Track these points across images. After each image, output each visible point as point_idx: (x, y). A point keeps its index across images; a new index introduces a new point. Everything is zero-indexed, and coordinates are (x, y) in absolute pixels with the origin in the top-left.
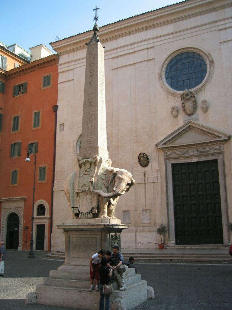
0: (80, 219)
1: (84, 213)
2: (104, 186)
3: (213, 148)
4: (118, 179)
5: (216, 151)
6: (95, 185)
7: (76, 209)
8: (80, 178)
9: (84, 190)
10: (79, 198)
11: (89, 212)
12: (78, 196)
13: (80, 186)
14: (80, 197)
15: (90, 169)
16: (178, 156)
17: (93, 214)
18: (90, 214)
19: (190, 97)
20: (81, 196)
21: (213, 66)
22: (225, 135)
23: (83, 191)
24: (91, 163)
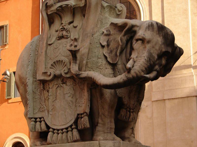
0: (50, 144)
1: (58, 130)
2: (104, 62)
4: (140, 42)
6: (81, 62)
7: (41, 122)
8: (49, 47)
9: (58, 72)
10: (46, 96)
11: (71, 126)
12: (44, 88)
13: (49, 66)
14: (48, 91)
15: (72, 24)
17: (80, 132)
18: (72, 131)
20: (50, 90)
23: (55, 75)
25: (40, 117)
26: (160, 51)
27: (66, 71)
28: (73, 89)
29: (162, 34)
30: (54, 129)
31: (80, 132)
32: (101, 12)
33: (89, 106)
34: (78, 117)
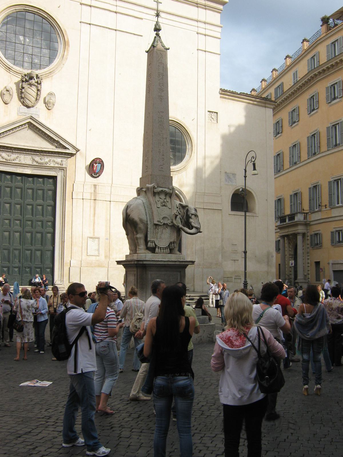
1: (161, 248)
3: (54, 161)
5: (56, 165)
9: (166, 222)
13: (161, 218)
16: (4, 160)
19: (35, 83)
20: (159, 229)
21: (68, 50)
22: (74, 147)
24: (166, 194)
27: (170, 223)
30: (159, 247)
31: (170, 249)
34: (171, 243)
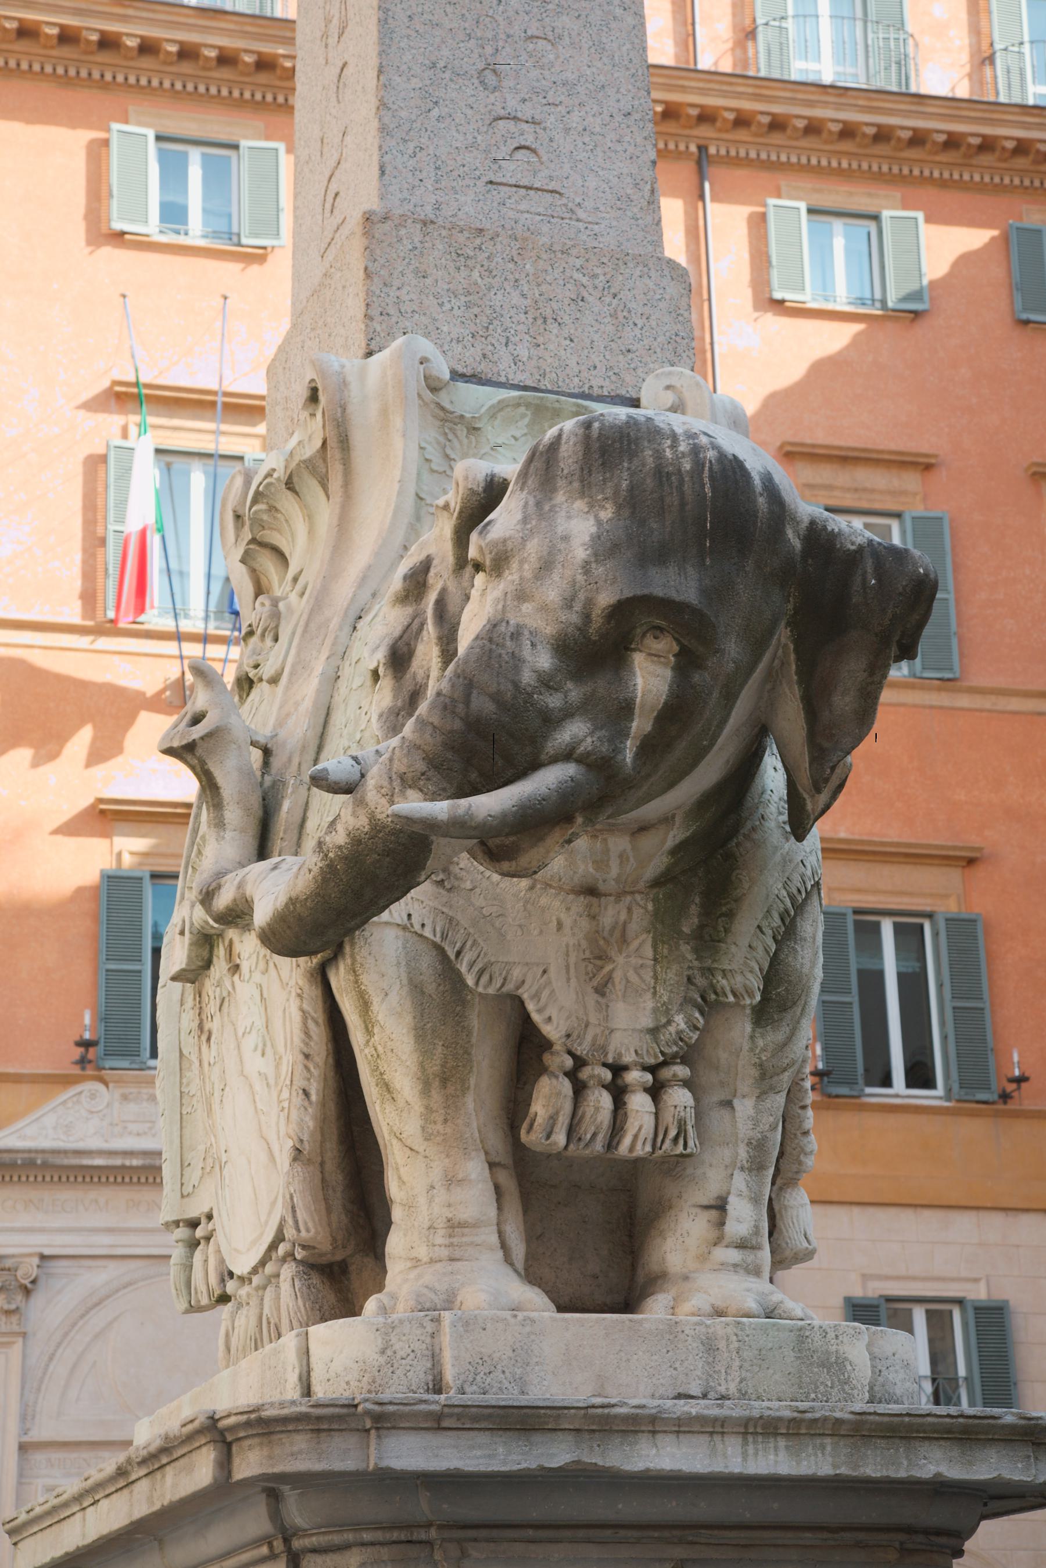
25: (206, 1210)
26: (578, 606)
28: (262, 995)
29: (617, 486)
32: (447, 456)
33: (306, 1093)
